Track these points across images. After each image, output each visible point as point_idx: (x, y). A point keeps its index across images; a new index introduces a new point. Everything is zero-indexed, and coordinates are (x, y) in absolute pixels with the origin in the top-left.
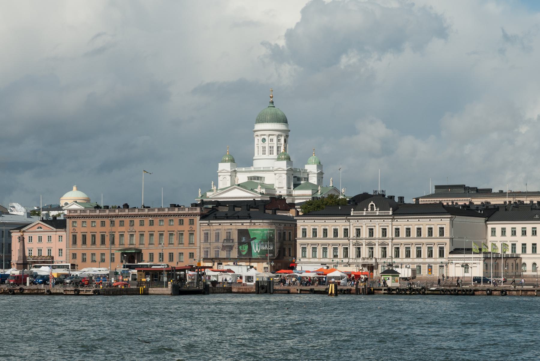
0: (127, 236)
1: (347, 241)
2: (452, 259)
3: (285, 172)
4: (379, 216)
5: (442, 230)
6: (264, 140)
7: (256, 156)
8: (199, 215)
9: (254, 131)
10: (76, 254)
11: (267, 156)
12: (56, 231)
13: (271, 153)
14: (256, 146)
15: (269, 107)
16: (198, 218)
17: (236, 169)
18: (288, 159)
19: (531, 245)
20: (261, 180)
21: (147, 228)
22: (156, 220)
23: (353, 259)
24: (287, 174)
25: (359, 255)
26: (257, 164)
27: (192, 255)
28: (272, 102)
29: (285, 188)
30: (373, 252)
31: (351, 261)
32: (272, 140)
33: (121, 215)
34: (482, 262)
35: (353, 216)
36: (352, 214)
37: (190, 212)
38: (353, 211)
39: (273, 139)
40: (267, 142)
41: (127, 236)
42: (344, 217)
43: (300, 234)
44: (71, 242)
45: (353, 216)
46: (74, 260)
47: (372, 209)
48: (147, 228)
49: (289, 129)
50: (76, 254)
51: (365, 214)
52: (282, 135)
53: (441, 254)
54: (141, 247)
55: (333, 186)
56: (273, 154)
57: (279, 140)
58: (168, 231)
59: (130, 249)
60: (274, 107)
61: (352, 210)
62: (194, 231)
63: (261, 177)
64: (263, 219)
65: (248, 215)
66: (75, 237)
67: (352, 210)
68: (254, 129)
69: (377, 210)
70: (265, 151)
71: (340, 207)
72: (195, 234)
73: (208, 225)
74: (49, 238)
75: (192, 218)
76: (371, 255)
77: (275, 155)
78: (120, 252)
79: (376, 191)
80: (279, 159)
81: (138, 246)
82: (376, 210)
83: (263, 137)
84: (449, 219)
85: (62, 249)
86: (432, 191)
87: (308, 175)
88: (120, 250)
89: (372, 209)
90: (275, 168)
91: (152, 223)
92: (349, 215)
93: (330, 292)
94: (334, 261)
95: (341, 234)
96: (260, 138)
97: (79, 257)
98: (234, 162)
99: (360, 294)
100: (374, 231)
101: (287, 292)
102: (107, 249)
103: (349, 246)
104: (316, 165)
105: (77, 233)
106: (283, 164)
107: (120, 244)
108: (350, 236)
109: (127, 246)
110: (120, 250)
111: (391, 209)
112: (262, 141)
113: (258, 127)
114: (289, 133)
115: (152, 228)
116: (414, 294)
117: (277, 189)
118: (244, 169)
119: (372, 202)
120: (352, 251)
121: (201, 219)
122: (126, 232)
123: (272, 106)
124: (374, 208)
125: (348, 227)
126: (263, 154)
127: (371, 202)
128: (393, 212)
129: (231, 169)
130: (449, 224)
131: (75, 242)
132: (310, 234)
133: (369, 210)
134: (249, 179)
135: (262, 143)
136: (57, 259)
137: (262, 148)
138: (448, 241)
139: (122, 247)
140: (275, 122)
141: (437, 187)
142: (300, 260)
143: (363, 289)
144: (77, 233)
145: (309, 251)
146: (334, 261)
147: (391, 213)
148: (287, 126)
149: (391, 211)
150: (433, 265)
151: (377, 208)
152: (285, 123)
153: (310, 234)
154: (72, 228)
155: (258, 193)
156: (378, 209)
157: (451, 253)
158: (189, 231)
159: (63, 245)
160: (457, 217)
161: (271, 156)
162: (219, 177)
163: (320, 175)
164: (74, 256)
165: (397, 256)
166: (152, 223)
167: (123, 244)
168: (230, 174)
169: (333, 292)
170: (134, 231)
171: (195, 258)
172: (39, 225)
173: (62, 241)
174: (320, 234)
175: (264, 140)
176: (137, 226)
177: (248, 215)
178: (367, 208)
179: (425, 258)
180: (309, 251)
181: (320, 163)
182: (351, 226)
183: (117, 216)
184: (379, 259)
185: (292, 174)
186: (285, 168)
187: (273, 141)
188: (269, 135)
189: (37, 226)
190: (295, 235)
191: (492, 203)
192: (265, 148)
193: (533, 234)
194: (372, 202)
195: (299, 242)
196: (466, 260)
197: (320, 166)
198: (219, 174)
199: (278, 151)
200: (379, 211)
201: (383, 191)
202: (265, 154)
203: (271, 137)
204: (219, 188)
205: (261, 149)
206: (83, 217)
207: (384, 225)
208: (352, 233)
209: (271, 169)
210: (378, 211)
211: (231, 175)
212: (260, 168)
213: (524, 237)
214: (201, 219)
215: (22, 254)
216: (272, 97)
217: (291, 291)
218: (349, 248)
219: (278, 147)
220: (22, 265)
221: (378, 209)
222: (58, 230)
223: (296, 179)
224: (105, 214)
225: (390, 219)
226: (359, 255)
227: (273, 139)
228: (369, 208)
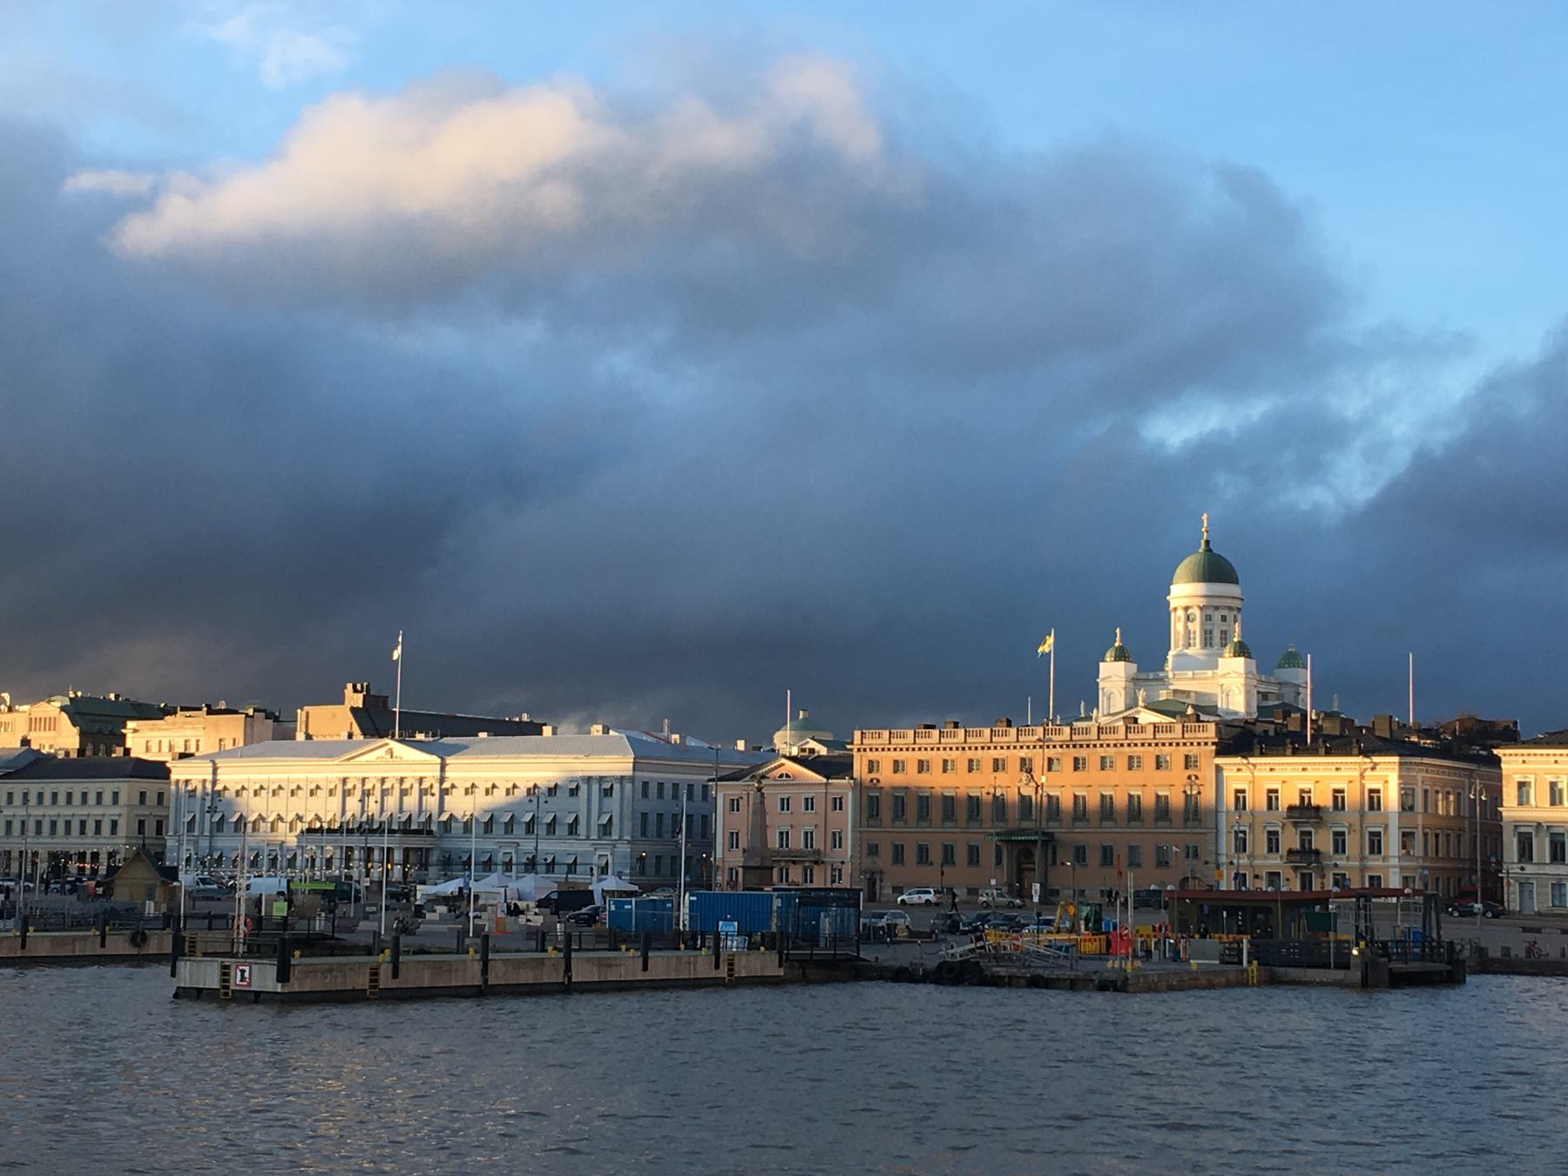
8: (1213, 744)
44: (865, 815)
59: (1023, 831)
70: (1195, 639)
97: (886, 853)
109: (1013, 824)
139: (1000, 827)
140: (1210, 581)
164: (873, 850)
198: (1101, 685)
214: (1219, 753)
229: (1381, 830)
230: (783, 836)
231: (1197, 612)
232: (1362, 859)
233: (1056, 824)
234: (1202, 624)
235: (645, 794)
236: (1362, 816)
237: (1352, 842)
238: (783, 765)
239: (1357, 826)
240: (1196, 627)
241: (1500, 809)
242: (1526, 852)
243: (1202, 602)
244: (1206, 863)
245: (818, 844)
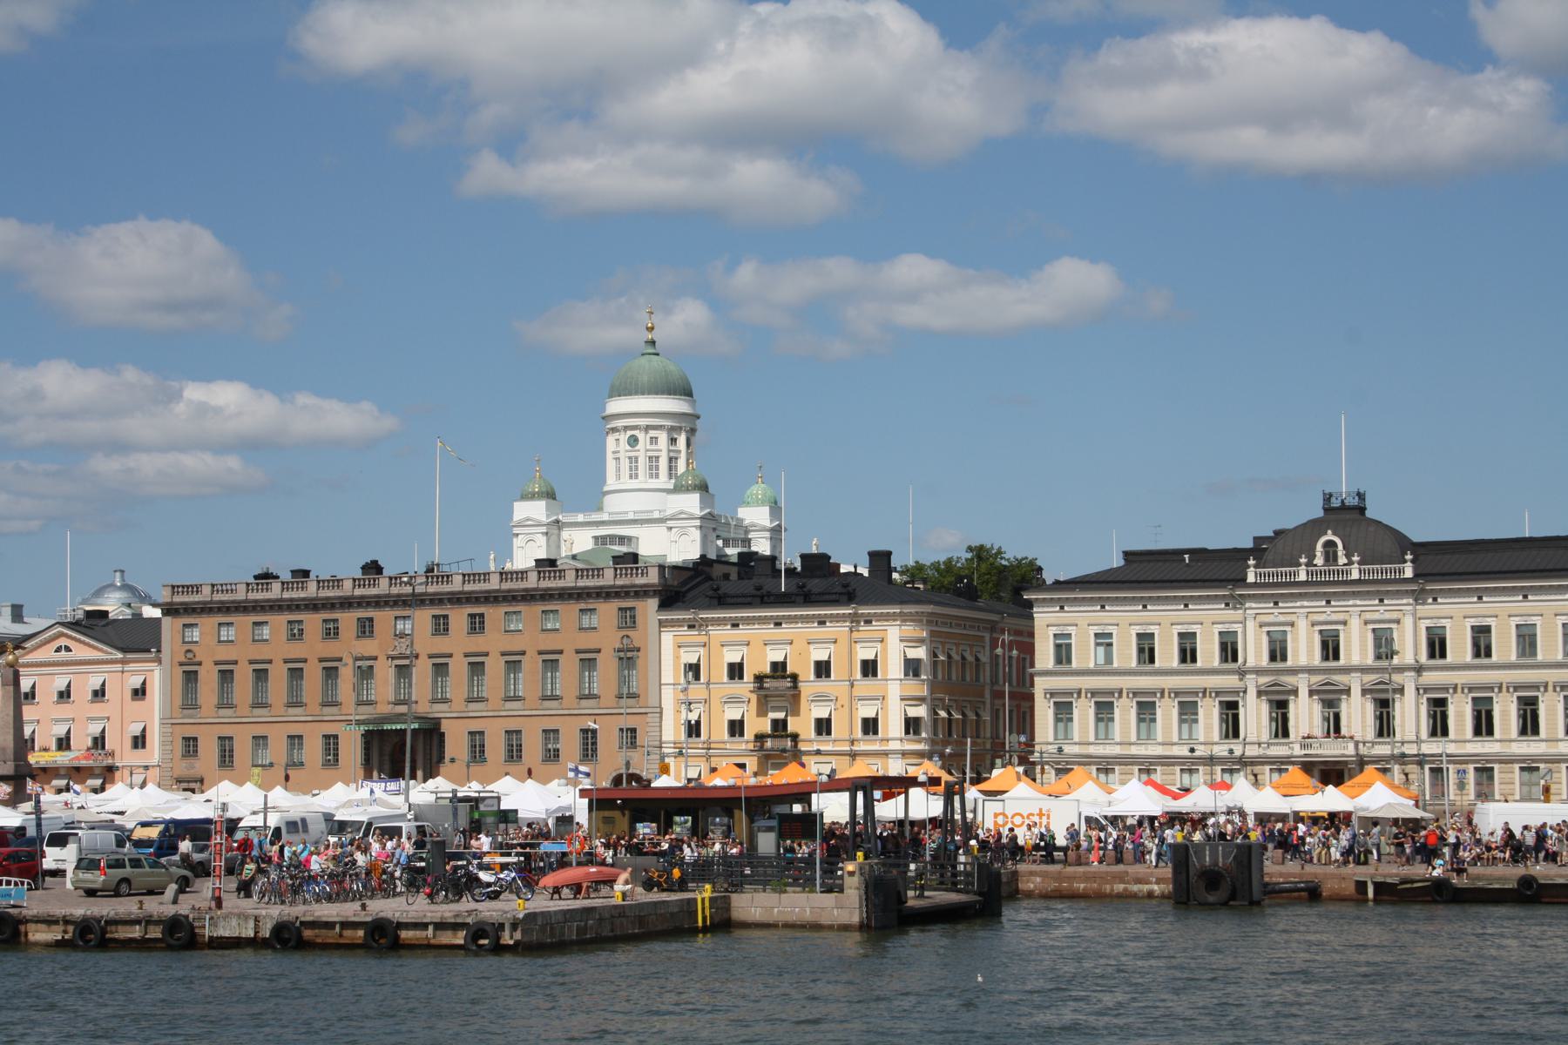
0: (385, 673)
1: (1231, 681)
4: (1358, 582)
6: (633, 441)
7: (611, 483)
9: (603, 418)
10: (195, 739)
11: (643, 481)
12: (123, 662)
13: (653, 472)
14: (610, 456)
15: (643, 355)
16: (653, 603)
17: (560, 517)
18: (703, 488)
20: (629, 545)
21: (459, 640)
22: (493, 614)
23: (1259, 744)
24: (701, 527)
25: (1282, 729)
26: (615, 505)
30: (1337, 717)
31: (1252, 751)
32: (654, 440)
33: (362, 597)
36: (1251, 578)
37: (619, 582)
38: (1256, 566)
39: (656, 438)
40: (640, 446)
41: (385, 673)
42: (1225, 587)
43: (1044, 656)
45: (1255, 585)
46: (192, 760)
47: (1331, 556)
48: (459, 640)
49: (698, 412)
50: (195, 739)
51: (1302, 577)
52: (681, 428)
54: (438, 711)
56: (657, 476)
57: (673, 441)
58: (540, 653)
59: (399, 718)
60: (658, 354)
61: (1251, 562)
62: (638, 650)
63: (630, 539)
64: (902, 602)
66: (191, 677)
67: (1251, 562)
68: (604, 410)
69: (1350, 563)
71: (1186, 556)
72: (639, 662)
76: (1334, 727)
77: (663, 481)
80: (677, 489)
81: (424, 708)
82: (1346, 561)
83: (630, 433)
86: (1117, 561)
87: (747, 532)
88: (359, 723)
89: (1331, 556)
90: (669, 513)
91: (477, 624)
92: (1241, 581)
95: (1208, 653)
96: (623, 437)
97: (209, 750)
98: (554, 499)
102: (310, 718)
103: (1244, 698)
104: (767, 508)
105: (200, 664)
106: (691, 503)
107: (360, 703)
108: (1245, 662)
109: (384, 709)
110: (359, 723)
112: (629, 444)
113: (616, 406)
114: (698, 422)
115: (478, 643)
118: (580, 518)
119: (1329, 532)
120: (1255, 717)
121: (665, 605)
122: (382, 659)
124: (1340, 553)
125: (1238, 628)
126: (631, 477)
127: (1326, 534)
128: (1415, 569)
129: (548, 516)
133: (1319, 560)
134: (596, 544)
135: (628, 448)
136: (126, 757)
137: (627, 460)
139: (366, 712)
140: (663, 393)
141: (1127, 554)
144: (200, 664)
146: (1197, 753)
147: (1409, 573)
148: (693, 403)
149: (1409, 564)
151: (1348, 556)
152: (685, 395)
156: (1356, 558)
161: (653, 483)
162: (515, 540)
163: (776, 533)
164: (190, 746)
165: (1439, 727)
166: (477, 624)
167: (370, 703)
172: (63, 642)
175: (633, 441)
178: (1312, 557)
181: (776, 503)
182: (1251, 625)
184: (1364, 743)
186: (698, 512)
187: (656, 443)
188: (648, 428)
192: (636, 458)
194: (1329, 532)
195: (1041, 685)
197: (775, 510)
199: (670, 468)
200: (1360, 563)
201: (1359, 494)
202: (637, 476)
203: (652, 433)
205: (625, 464)
207: (1329, 619)
208: (1254, 651)
209: (656, 515)
210: (1356, 565)
211: (547, 533)
212: (626, 513)
214: (665, 605)
216: (652, 328)
218: (1241, 704)
219: (670, 459)
221: (1356, 558)
222: (130, 656)
224: (302, 595)
225: (1406, 593)
226: (1282, 729)
227: (656, 438)
228: (1318, 554)
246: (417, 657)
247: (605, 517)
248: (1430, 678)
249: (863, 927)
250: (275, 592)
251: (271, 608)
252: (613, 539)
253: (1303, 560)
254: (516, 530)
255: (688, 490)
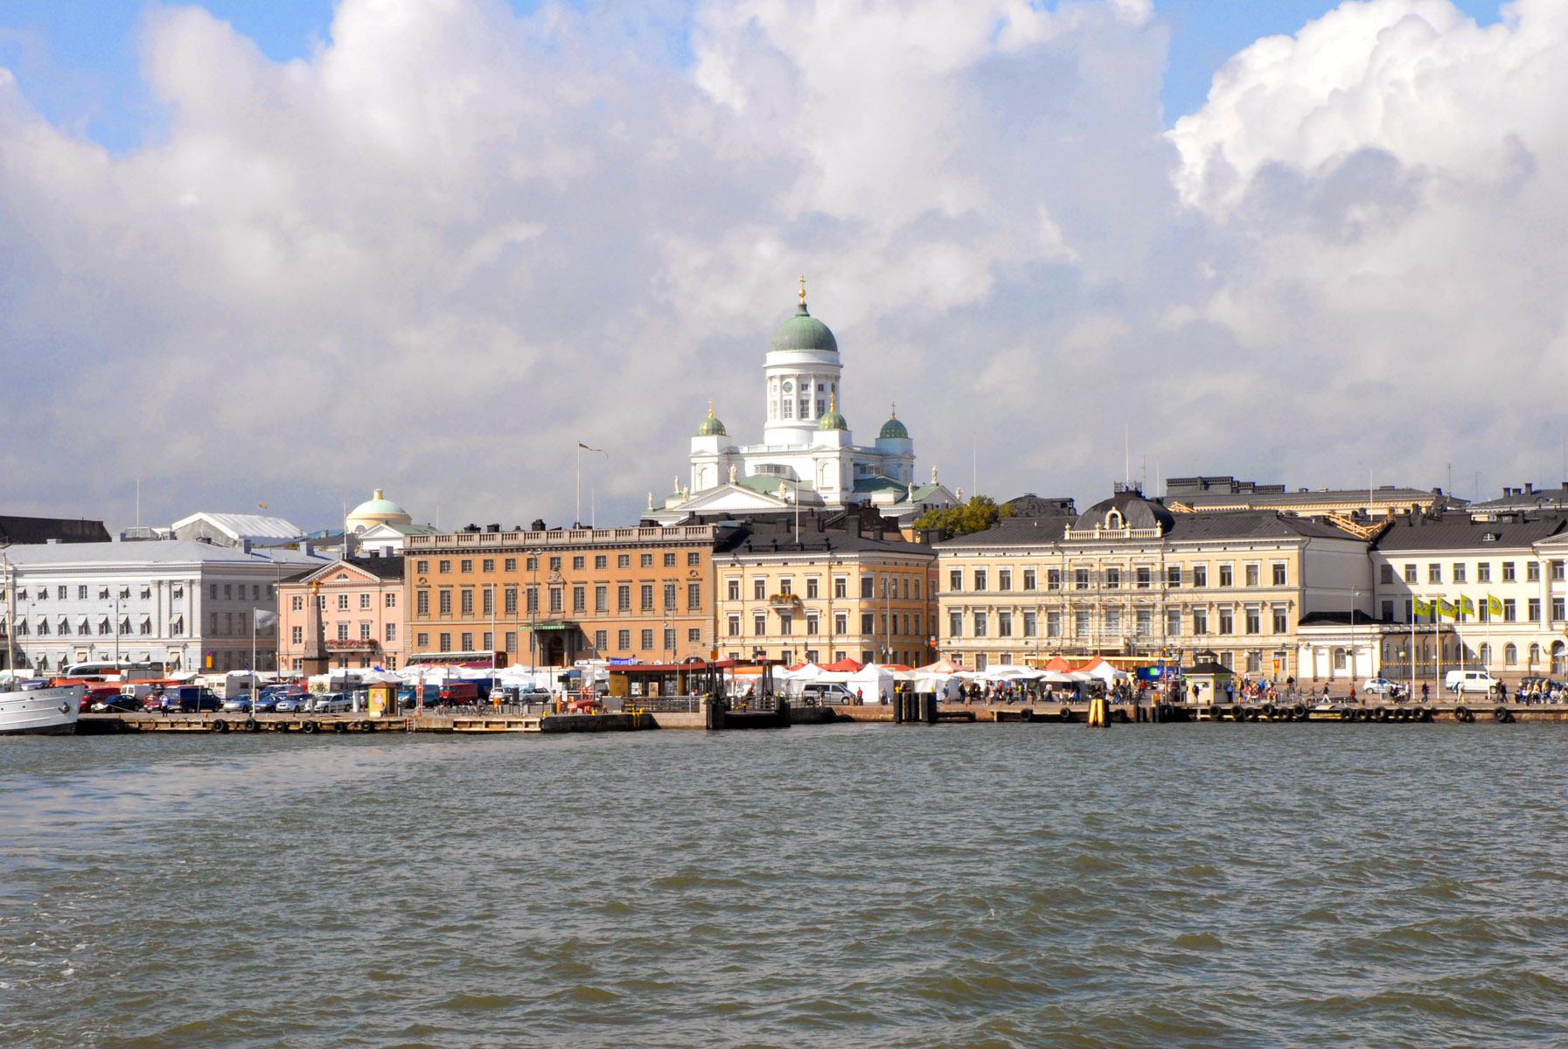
2: (1310, 637)
3: (837, 454)
4: (1130, 539)
5: (1279, 574)
12: (380, 585)
13: (803, 413)
16: (711, 549)
19: (1527, 601)
21: (589, 573)
27: (694, 635)
28: (804, 306)
29: (837, 489)
32: (805, 387)
34: (1377, 644)
35: (1070, 541)
36: (1067, 537)
38: (1070, 529)
45: (1070, 541)
47: (1113, 524)
48: (589, 573)
51: (1097, 536)
53: (1280, 625)
54: (578, 618)
55: (938, 485)
59: (553, 622)
60: (808, 315)
61: (1067, 527)
64: (860, 551)
65: (825, 542)
69: (1125, 528)
70: (790, 409)
73: (733, 565)
74: (364, 599)
75: (695, 550)
78: (530, 629)
79: (1121, 484)
81: (570, 616)
84: (1297, 547)
85: (394, 625)
89: (1113, 524)
93: (1091, 720)
94: (1030, 645)
99: (1146, 720)
100: (1286, 570)
101: (966, 718)
105: (430, 587)
110: (529, 625)
111: (1159, 524)
116: (1275, 721)
117: (820, 492)
123: (804, 313)
130: (1296, 556)
131: (422, 606)
132: (968, 583)
133: (1107, 526)
138: (1295, 596)
142: (949, 643)
143: (1154, 709)
144: (430, 587)
145: (968, 622)
147: (1158, 532)
150: (1233, 652)
151: (1124, 521)
153: (968, 583)
154: (416, 577)
155: (781, 500)
156: (1127, 525)
157: (1302, 622)
158: (688, 580)
159: (397, 614)
160: (1313, 539)
162: (693, 468)
164: (422, 640)
168: (716, 460)
169: (1100, 719)
170: (560, 580)
171: (702, 639)
173: (394, 605)
174: (993, 583)
176: (568, 573)
177: (825, 542)
179: (1239, 636)
180: (968, 622)
183: (521, 549)
185: (851, 460)
189: (338, 573)
190: (934, 585)
191: (1301, 515)
192: (790, 403)
193: (1506, 577)
195: (943, 604)
196: (1358, 639)
204: (692, 491)
206: (444, 551)
209: (805, 448)
213: (1509, 585)
215: (316, 636)
217: (978, 715)
220: (317, 662)
222: (386, 581)
223: (858, 468)
229: (739, 615)
230: (342, 628)
231: (793, 382)
232: (831, 637)
233: (582, 615)
234: (799, 394)
235: (214, 596)
236: (830, 603)
237: (823, 625)
238: (341, 568)
239: (826, 611)
240: (793, 396)
241: (937, 594)
242: (955, 629)
243: (796, 372)
244: (704, 645)
245: (374, 635)
246: (565, 583)
247: (765, 450)
248: (1171, 599)
249: (708, 728)
250: (475, 541)
251: (474, 551)
252: (770, 467)
253: (1097, 525)
254: (693, 460)
255: (829, 428)
